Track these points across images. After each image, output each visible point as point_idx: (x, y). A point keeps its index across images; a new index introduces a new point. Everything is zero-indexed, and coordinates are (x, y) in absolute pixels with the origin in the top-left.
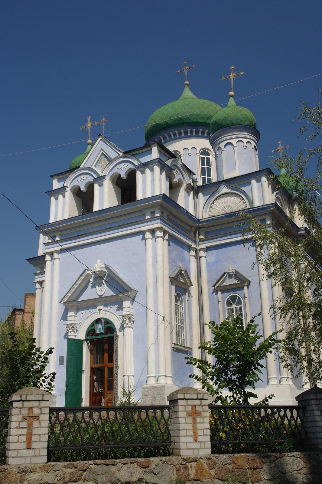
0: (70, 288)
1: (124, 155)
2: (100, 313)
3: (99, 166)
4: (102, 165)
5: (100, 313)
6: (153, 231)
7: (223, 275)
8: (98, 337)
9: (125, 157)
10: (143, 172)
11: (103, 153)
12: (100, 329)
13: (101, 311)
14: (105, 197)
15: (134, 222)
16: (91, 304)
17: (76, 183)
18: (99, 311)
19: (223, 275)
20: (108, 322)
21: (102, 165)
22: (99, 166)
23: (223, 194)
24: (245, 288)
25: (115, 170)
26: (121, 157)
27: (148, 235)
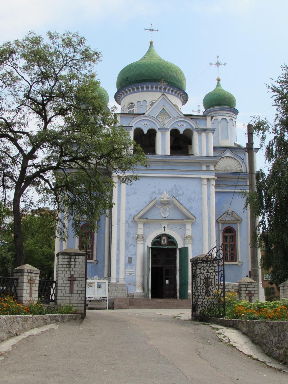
0: (142, 209)
1: (184, 117)
2: (164, 230)
3: (160, 118)
4: (163, 118)
5: (164, 230)
6: (208, 180)
7: (224, 214)
8: (161, 247)
9: (185, 118)
10: (200, 134)
11: (163, 108)
12: (164, 242)
13: (165, 229)
14: (163, 144)
15: (195, 170)
16: (158, 222)
17: (139, 126)
18: (164, 229)
19: (224, 214)
20: (169, 237)
21: (163, 118)
22: (160, 118)
23: (226, 157)
24: (238, 224)
25: (176, 126)
26: (182, 118)
27: (205, 182)
